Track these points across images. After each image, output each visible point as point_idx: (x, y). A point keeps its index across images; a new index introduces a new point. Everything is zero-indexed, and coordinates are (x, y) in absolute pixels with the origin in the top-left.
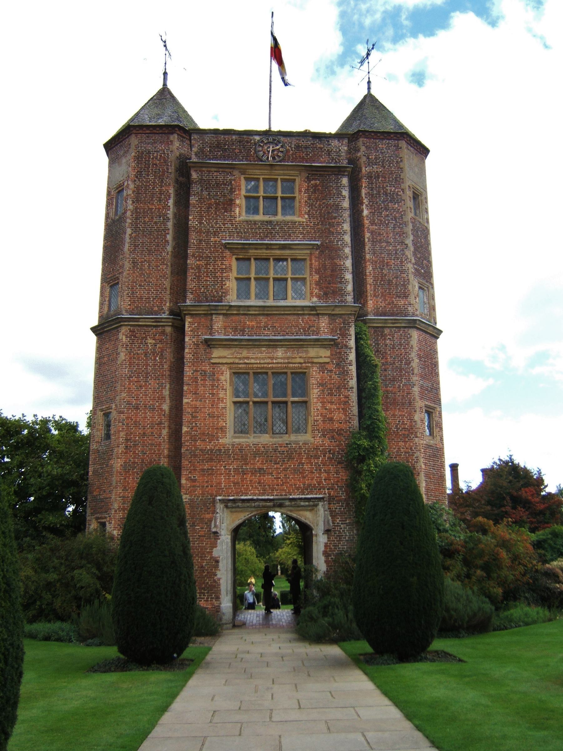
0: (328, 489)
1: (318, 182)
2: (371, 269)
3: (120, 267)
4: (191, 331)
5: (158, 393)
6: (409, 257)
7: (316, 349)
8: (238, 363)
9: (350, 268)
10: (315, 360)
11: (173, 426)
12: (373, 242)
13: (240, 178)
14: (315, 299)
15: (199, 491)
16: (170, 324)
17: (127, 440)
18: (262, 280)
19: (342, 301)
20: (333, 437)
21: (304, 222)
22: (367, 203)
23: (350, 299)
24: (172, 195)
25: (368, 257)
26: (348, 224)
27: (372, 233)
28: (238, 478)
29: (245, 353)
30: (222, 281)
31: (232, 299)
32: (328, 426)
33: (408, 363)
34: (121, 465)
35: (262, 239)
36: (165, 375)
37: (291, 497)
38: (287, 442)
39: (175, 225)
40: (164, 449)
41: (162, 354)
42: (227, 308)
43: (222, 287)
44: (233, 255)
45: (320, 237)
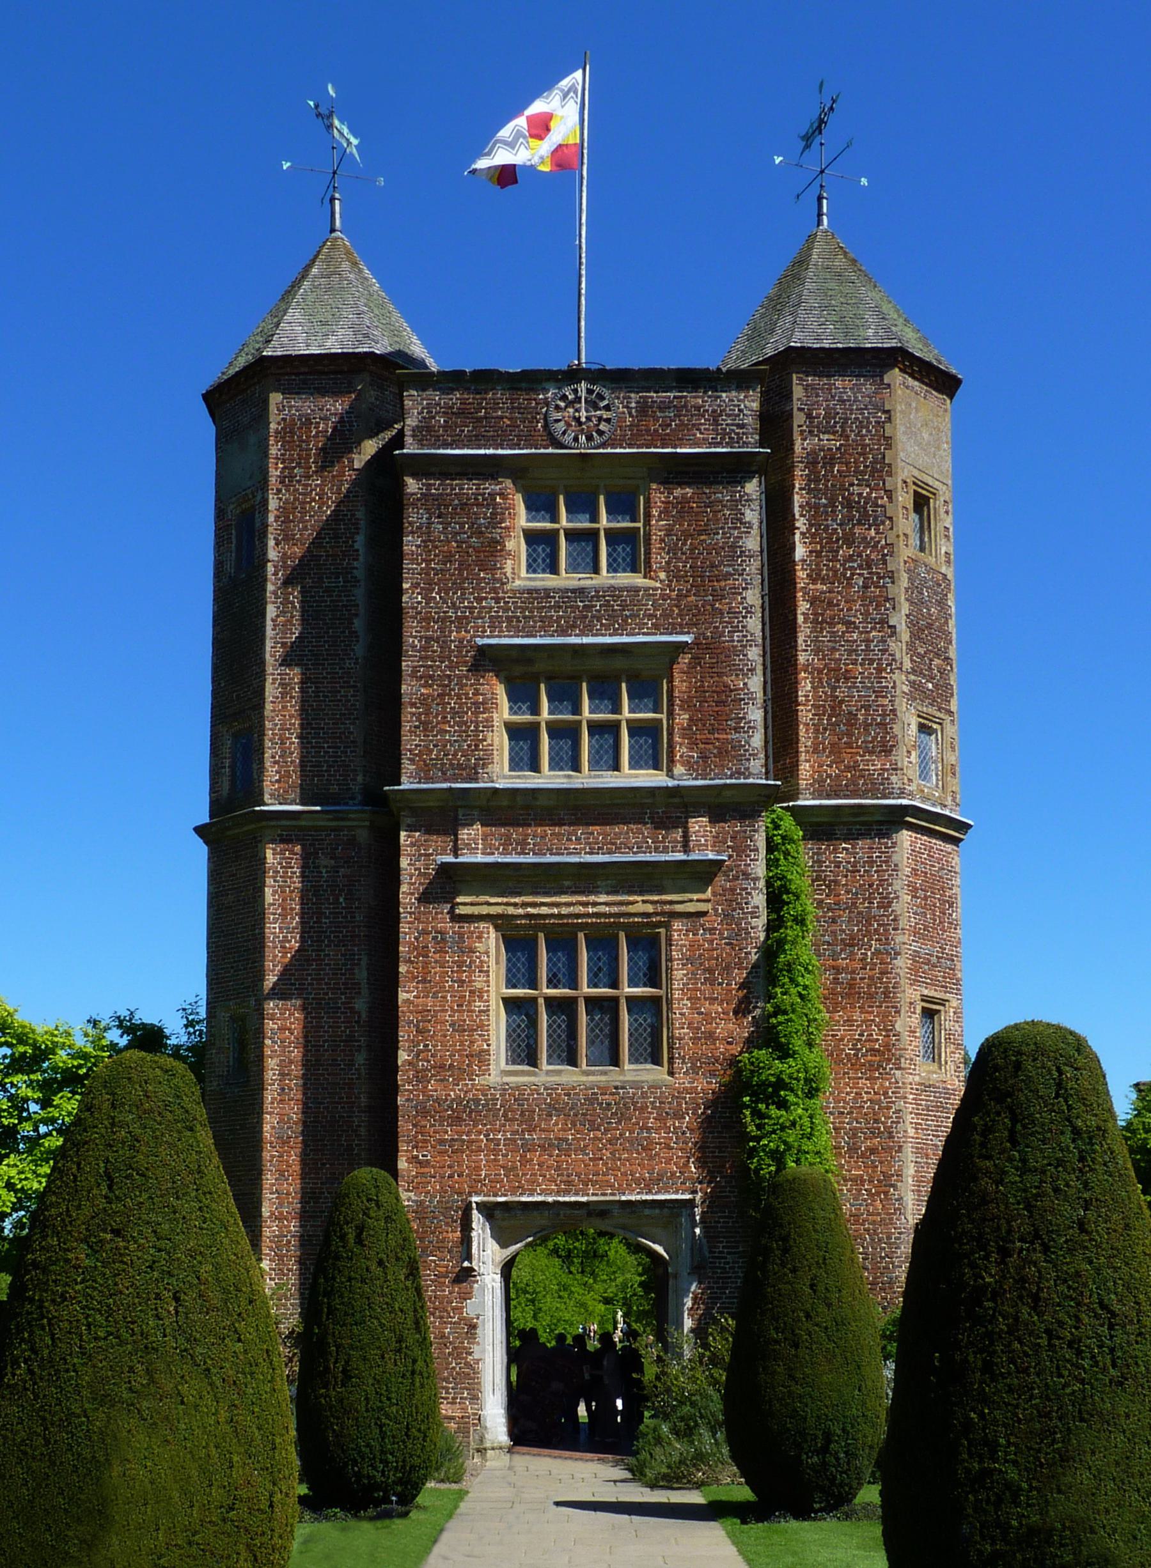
4: (412, 845)
5: (344, 974)
6: (898, 656)
9: (760, 695)
12: (817, 624)
15: (434, 1186)
16: (367, 823)
18: (565, 734)
19: (738, 773)
21: (655, 589)
22: (804, 529)
23: (757, 765)
25: (802, 658)
26: (757, 591)
27: (813, 601)
30: (476, 730)
31: (502, 774)
33: (886, 903)
35: (563, 632)
37: (623, 1198)
38: (619, 1084)
40: (359, 1093)
43: (477, 746)
45: (691, 625)
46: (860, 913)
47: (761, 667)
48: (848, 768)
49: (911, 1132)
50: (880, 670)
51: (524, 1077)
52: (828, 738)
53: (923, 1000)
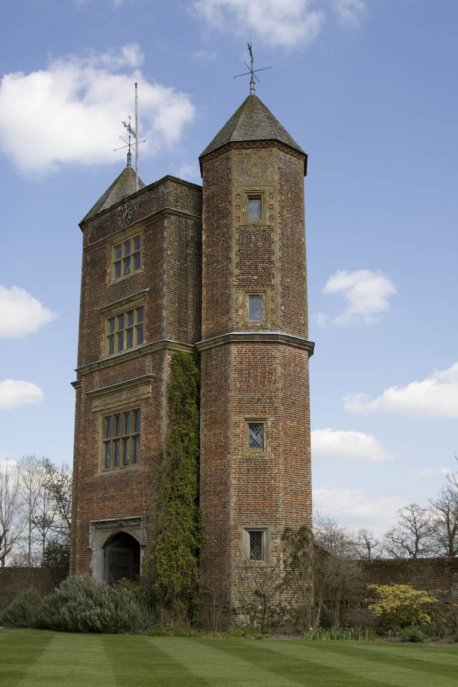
0: (146, 510)
19: (161, 338)
29: (108, 400)
49: (234, 482)
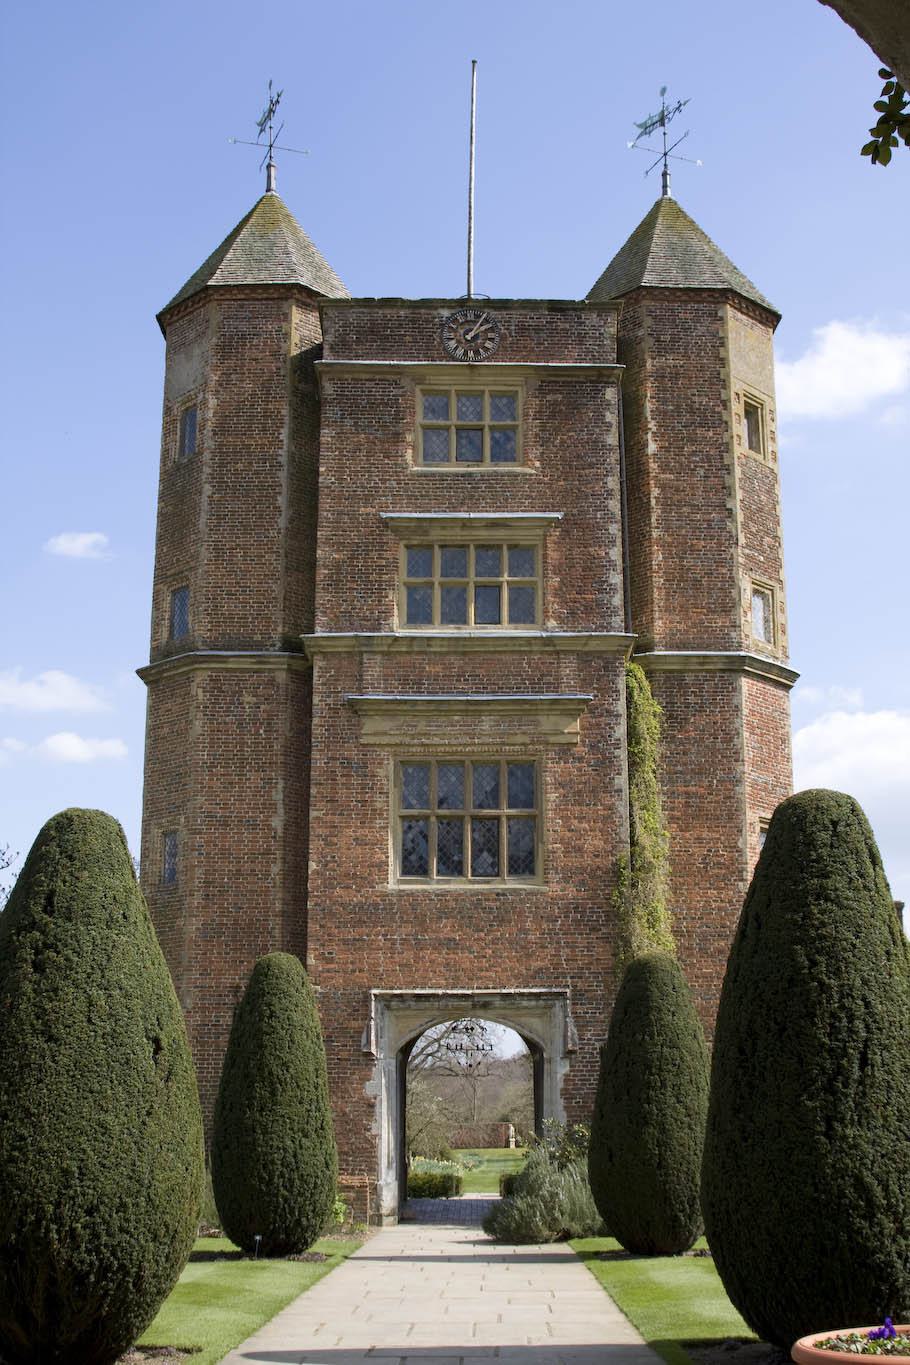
0: (572, 978)
1: (559, 397)
2: (661, 558)
3: (192, 556)
4: (323, 684)
5: (263, 796)
7: (552, 718)
8: (409, 745)
9: (619, 562)
10: (552, 739)
11: (290, 858)
12: (666, 504)
13: (413, 392)
14: (552, 623)
17: (207, 883)
19: (602, 628)
20: (583, 883)
21: (531, 475)
22: (654, 429)
23: (618, 620)
24: (287, 420)
25: (655, 534)
26: (616, 478)
27: (663, 487)
28: (409, 956)
32: (574, 861)
34: (198, 929)
36: (276, 763)
38: (500, 891)
39: (291, 476)
41: (269, 724)
42: (390, 641)
44: (401, 539)
46: (707, 747)
47: (620, 540)
48: (694, 625)
50: (720, 544)
51: (415, 886)
52: (678, 600)
53: (761, 822)
